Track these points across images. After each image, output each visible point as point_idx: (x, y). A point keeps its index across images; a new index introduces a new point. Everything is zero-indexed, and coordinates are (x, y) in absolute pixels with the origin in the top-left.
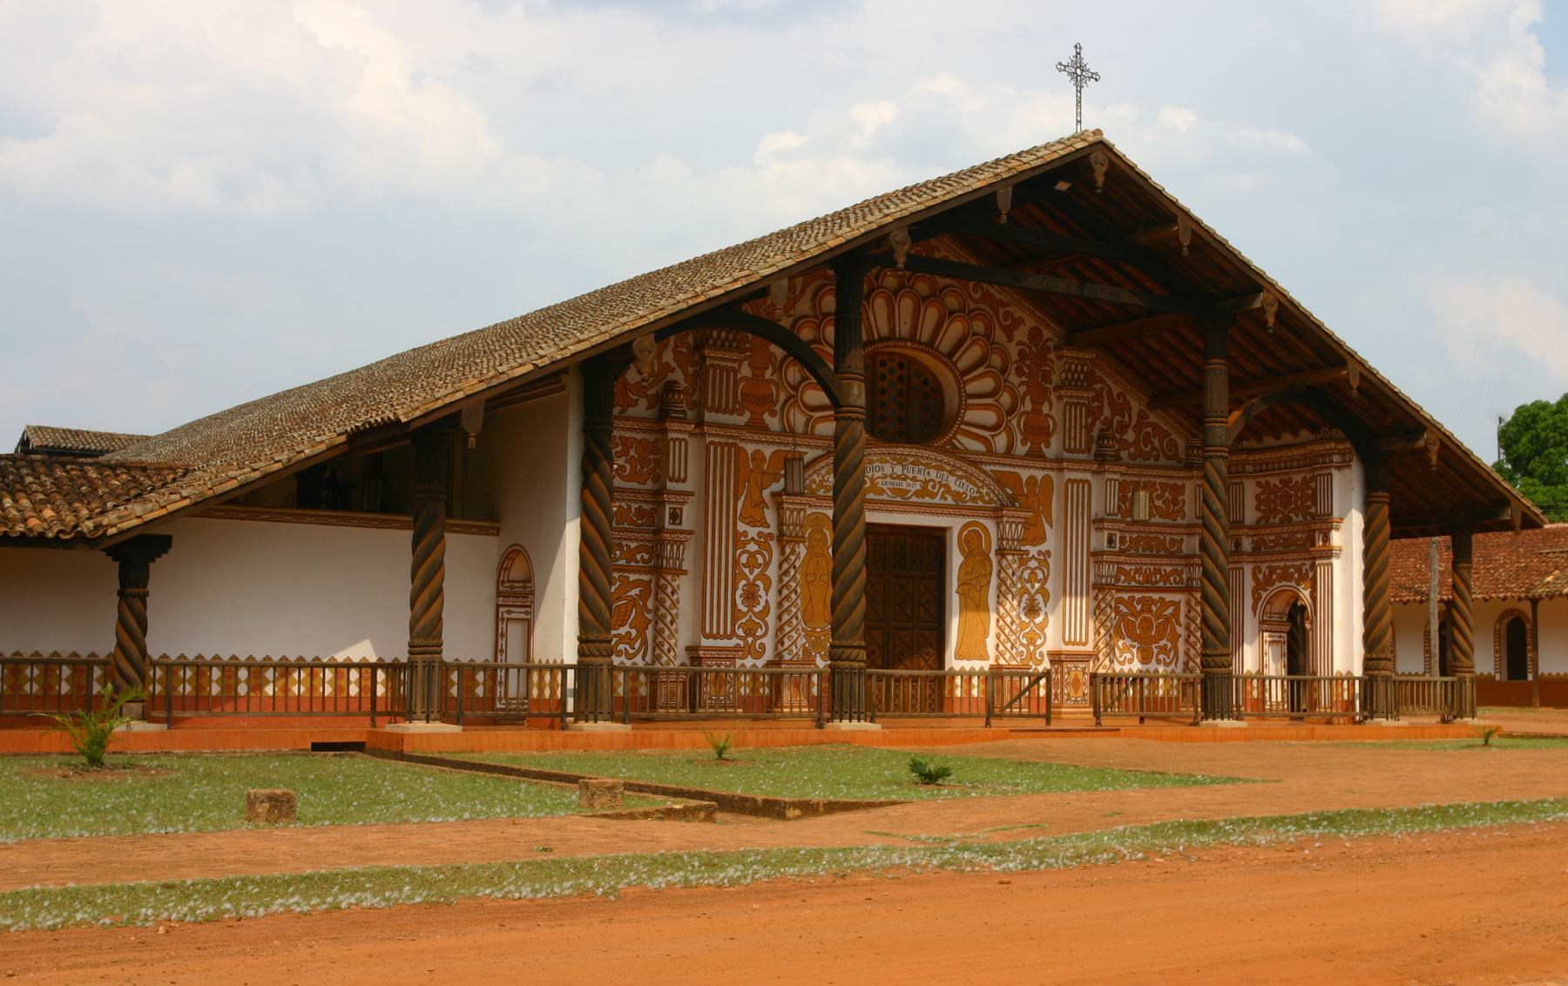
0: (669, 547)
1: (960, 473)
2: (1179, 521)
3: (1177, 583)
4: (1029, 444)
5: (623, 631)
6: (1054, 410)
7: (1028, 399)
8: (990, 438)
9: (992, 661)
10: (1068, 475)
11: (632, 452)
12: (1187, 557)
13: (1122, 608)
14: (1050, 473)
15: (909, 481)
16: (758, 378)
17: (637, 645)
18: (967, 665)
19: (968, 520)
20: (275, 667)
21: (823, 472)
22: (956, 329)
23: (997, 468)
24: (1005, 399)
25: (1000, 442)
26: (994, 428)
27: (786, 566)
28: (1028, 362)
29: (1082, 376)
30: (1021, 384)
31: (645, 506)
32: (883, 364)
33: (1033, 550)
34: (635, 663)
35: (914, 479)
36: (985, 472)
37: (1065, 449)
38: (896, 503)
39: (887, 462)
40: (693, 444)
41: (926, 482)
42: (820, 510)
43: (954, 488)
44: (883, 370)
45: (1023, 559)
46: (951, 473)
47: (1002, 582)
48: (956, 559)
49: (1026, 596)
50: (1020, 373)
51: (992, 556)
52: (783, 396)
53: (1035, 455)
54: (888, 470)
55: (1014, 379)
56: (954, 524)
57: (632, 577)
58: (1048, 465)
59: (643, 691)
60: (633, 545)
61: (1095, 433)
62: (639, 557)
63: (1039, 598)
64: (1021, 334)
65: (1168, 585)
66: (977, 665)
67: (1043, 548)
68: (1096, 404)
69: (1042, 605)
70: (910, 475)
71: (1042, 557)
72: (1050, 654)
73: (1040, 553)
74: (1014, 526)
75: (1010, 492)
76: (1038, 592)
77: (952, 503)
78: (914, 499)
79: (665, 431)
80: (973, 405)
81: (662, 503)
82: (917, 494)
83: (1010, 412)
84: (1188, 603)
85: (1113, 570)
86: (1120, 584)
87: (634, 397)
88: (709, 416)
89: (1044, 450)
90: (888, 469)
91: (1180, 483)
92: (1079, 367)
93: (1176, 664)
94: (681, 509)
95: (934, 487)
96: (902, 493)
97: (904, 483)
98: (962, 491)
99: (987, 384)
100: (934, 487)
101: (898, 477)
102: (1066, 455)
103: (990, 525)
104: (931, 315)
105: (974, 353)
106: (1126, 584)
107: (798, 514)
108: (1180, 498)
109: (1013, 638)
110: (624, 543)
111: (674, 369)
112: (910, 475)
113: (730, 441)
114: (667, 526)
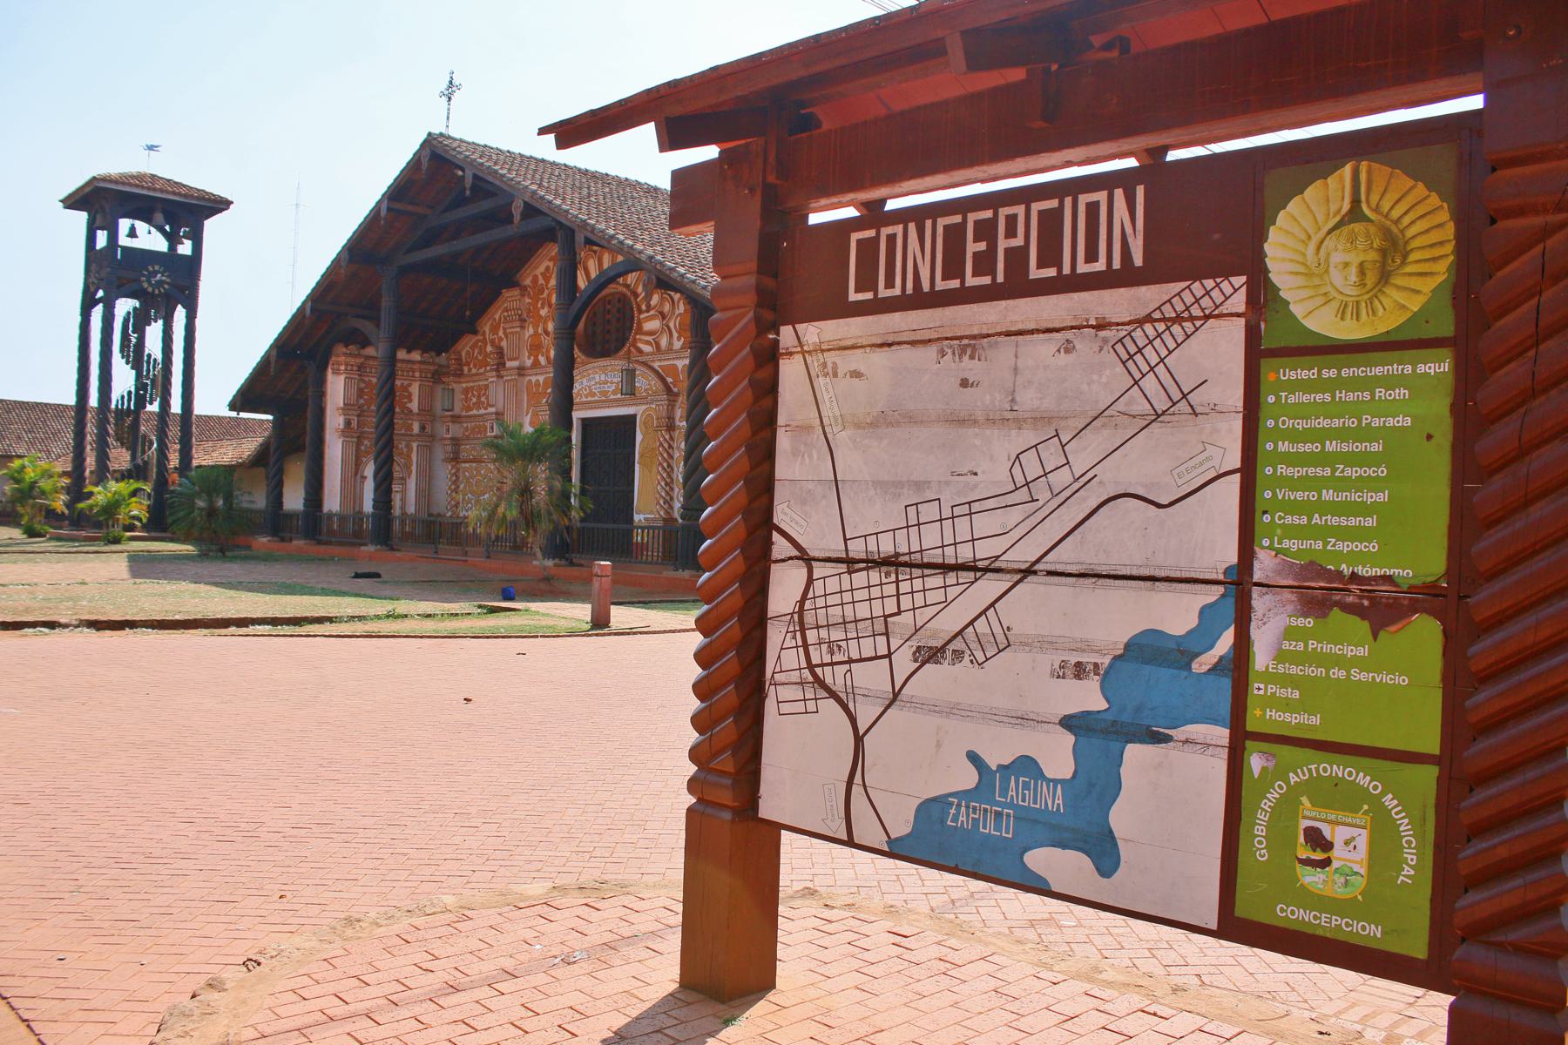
4: (683, 339)
7: (681, 302)
16: (536, 333)
23: (663, 363)
32: (609, 303)
35: (612, 383)
38: (603, 401)
44: (608, 307)
48: (639, 437)
54: (597, 380)
78: (612, 397)
80: (643, 319)
96: (604, 393)
112: (609, 380)
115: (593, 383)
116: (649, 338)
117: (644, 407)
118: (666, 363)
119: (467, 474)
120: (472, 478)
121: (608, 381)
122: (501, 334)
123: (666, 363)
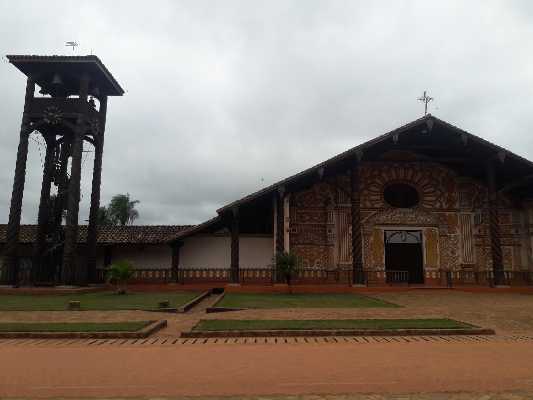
0: (329, 239)
1: (424, 215)
2: (508, 224)
3: (509, 243)
5: (318, 260)
6: (456, 195)
8: (433, 204)
9: (439, 267)
10: (462, 213)
11: (319, 215)
12: (512, 235)
13: (487, 251)
14: (456, 213)
15: (406, 218)
17: (323, 264)
18: (430, 269)
19: (428, 228)
20: (199, 270)
21: (377, 217)
22: (419, 175)
23: (437, 212)
24: (439, 193)
25: (438, 205)
26: (435, 201)
27: (366, 243)
28: (446, 182)
29: (465, 184)
30: (443, 189)
31: (323, 229)
33: (452, 235)
34: (322, 269)
36: (432, 214)
37: (460, 205)
38: (402, 224)
39: (398, 213)
40: (335, 213)
41: (412, 218)
42: (377, 227)
43: (422, 219)
45: (449, 238)
46: (420, 215)
47: (440, 245)
49: (451, 249)
50: (443, 185)
51: (437, 237)
52: (363, 198)
53: (451, 208)
55: (441, 187)
56: (424, 229)
57: (321, 247)
58: (455, 211)
59: (439, 277)
60: (320, 238)
61: (473, 200)
62: (322, 241)
63: (455, 249)
64: (443, 174)
65: (505, 243)
66: (434, 269)
67: (456, 234)
68: (472, 192)
69: (456, 251)
70: (406, 216)
71: (456, 237)
72: (461, 265)
73: (455, 236)
74: (443, 229)
75: (441, 219)
76: (455, 247)
77: (422, 223)
78: (408, 223)
79: (326, 210)
80: (426, 196)
81: (326, 228)
82: (409, 221)
83: (440, 196)
84: (514, 249)
85: (481, 240)
86: (486, 244)
87: (319, 202)
88: (339, 205)
89: (454, 206)
90: (398, 215)
91: (507, 213)
92: (464, 182)
93: (511, 268)
94: (332, 229)
95: (415, 219)
97: (405, 219)
98: (425, 220)
99: (432, 189)
100: (415, 219)
101: (402, 217)
102: (461, 207)
103: (436, 229)
104: (411, 172)
105: (427, 181)
106: (488, 244)
107: (369, 228)
108: (508, 217)
109: (445, 261)
110: (318, 238)
111: (330, 194)
112: (406, 216)
113: (346, 211)
114: (328, 233)
115: (395, 217)
116: (432, 203)
117: (426, 228)
118: (439, 212)
119: (303, 250)
120: (306, 252)
121: (405, 217)
122: (328, 191)
123: (439, 212)
